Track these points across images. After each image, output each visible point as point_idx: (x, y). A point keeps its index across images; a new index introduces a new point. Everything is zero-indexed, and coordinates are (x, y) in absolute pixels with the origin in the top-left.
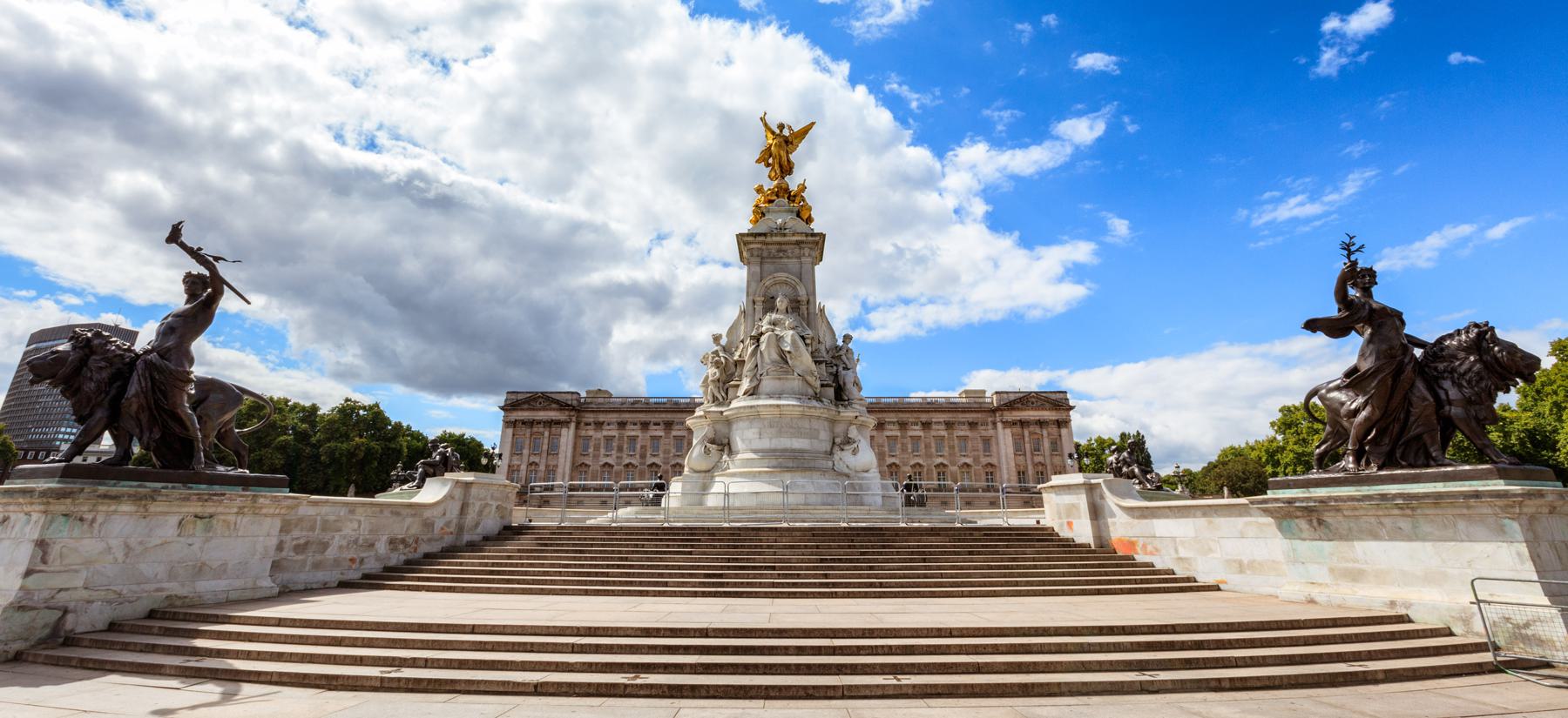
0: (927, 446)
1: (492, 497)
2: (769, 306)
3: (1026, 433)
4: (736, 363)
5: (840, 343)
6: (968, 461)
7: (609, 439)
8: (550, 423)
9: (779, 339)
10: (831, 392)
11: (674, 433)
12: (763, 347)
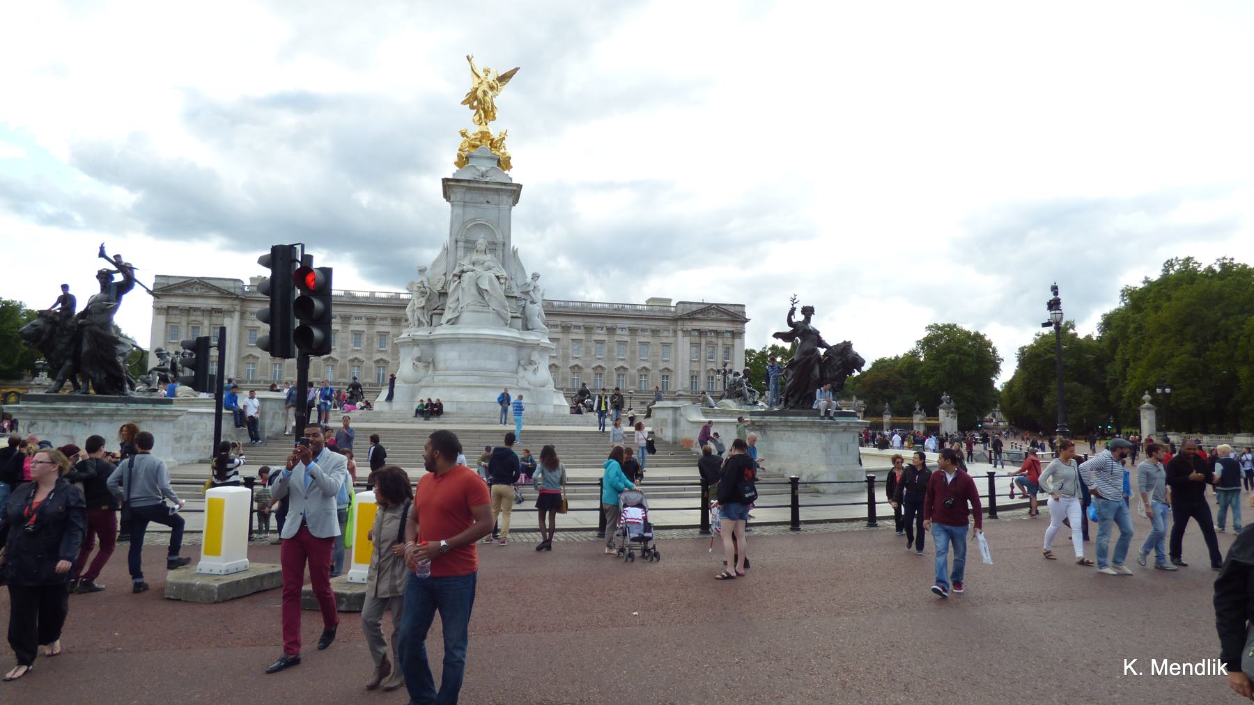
0: (610, 350)
5: (529, 280)
6: (647, 365)
10: (519, 322)
11: (352, 328)
12: (464, 284)
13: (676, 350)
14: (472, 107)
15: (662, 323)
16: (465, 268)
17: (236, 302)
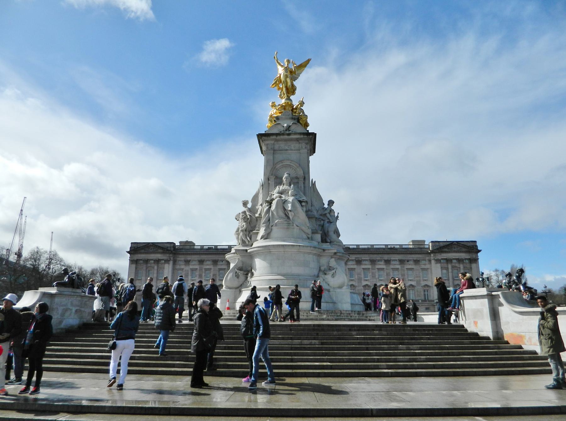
1: (72, 304)
2: (279, 182)
3: (450, 266)
4: (257, 218)
5: (326, 206)
6: (413, 283)
7: (192, 270)
8: (157, 261)
9: (285, 202)
13: (431, 273)
14: (279, 88)
15: (420, 256)
16: (274, 197)
17: (171, 255)
